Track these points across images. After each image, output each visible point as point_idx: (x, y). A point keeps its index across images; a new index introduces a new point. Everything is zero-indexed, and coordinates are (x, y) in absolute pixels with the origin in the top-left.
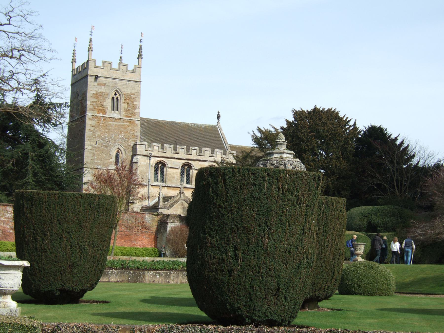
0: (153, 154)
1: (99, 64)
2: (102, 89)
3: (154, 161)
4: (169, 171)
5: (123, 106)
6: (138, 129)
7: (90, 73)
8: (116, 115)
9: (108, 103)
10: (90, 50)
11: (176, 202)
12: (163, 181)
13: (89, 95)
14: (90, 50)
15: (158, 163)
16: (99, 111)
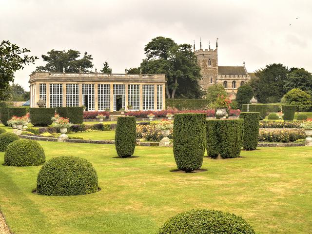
0: (223, 79)
1: (204, 50)
2: (205, 59)
3: (223, 81)
4: (228, 84)
5: (212, 63)
6: (217, 71)
8: (210, 67)
9: (207, 63)
10: (201, 46)
14: (201, 46)
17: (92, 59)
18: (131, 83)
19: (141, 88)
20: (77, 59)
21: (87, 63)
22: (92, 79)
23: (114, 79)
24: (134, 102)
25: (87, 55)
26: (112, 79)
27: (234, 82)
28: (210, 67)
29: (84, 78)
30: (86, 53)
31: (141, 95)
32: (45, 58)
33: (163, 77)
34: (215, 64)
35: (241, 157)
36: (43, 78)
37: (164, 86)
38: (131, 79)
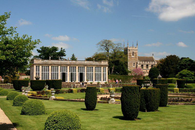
2: (130, 52)
3: (141, 65)
5: (134, 55)
6: (137, 59)
7: (128, 49)
8: (133, 57)
9: (132, 55)
11: (146, 73)
12: (142, 69)
13: (128, 53)
15: (141, 65)
16: (130, 56)
17: (65, 51)
18: (88, 66)
19: (94, 68)
20: (57, 52)
21: (62, 54)
22: (66, 63)
23: (78, 64)
24: (90, 77)
25: (62, 49)
26: (77, 64)
27: (147, 66)
28: (133, 57)
29: (61, 63)
30: (62, 48)
31: (94, 72)
32: (39, 51)
33: (106, 63)
34: (136, 56)
35: (158, 111)
36: (38, 63)
37: (107, 67)
38: (88, 64)
